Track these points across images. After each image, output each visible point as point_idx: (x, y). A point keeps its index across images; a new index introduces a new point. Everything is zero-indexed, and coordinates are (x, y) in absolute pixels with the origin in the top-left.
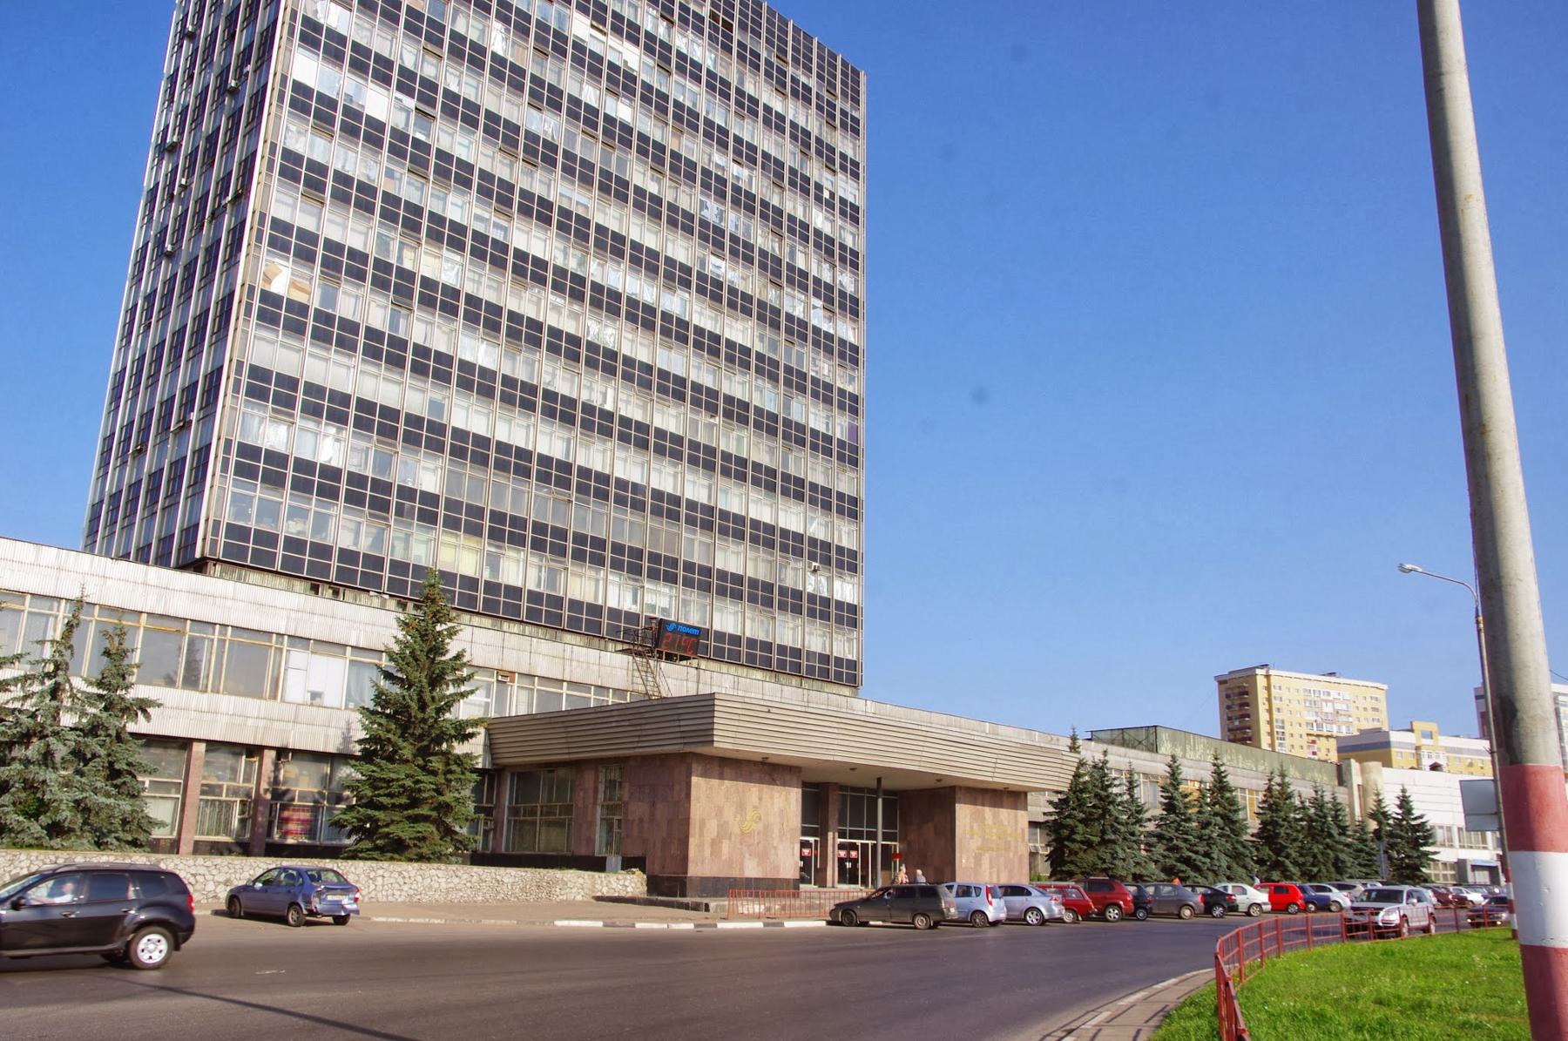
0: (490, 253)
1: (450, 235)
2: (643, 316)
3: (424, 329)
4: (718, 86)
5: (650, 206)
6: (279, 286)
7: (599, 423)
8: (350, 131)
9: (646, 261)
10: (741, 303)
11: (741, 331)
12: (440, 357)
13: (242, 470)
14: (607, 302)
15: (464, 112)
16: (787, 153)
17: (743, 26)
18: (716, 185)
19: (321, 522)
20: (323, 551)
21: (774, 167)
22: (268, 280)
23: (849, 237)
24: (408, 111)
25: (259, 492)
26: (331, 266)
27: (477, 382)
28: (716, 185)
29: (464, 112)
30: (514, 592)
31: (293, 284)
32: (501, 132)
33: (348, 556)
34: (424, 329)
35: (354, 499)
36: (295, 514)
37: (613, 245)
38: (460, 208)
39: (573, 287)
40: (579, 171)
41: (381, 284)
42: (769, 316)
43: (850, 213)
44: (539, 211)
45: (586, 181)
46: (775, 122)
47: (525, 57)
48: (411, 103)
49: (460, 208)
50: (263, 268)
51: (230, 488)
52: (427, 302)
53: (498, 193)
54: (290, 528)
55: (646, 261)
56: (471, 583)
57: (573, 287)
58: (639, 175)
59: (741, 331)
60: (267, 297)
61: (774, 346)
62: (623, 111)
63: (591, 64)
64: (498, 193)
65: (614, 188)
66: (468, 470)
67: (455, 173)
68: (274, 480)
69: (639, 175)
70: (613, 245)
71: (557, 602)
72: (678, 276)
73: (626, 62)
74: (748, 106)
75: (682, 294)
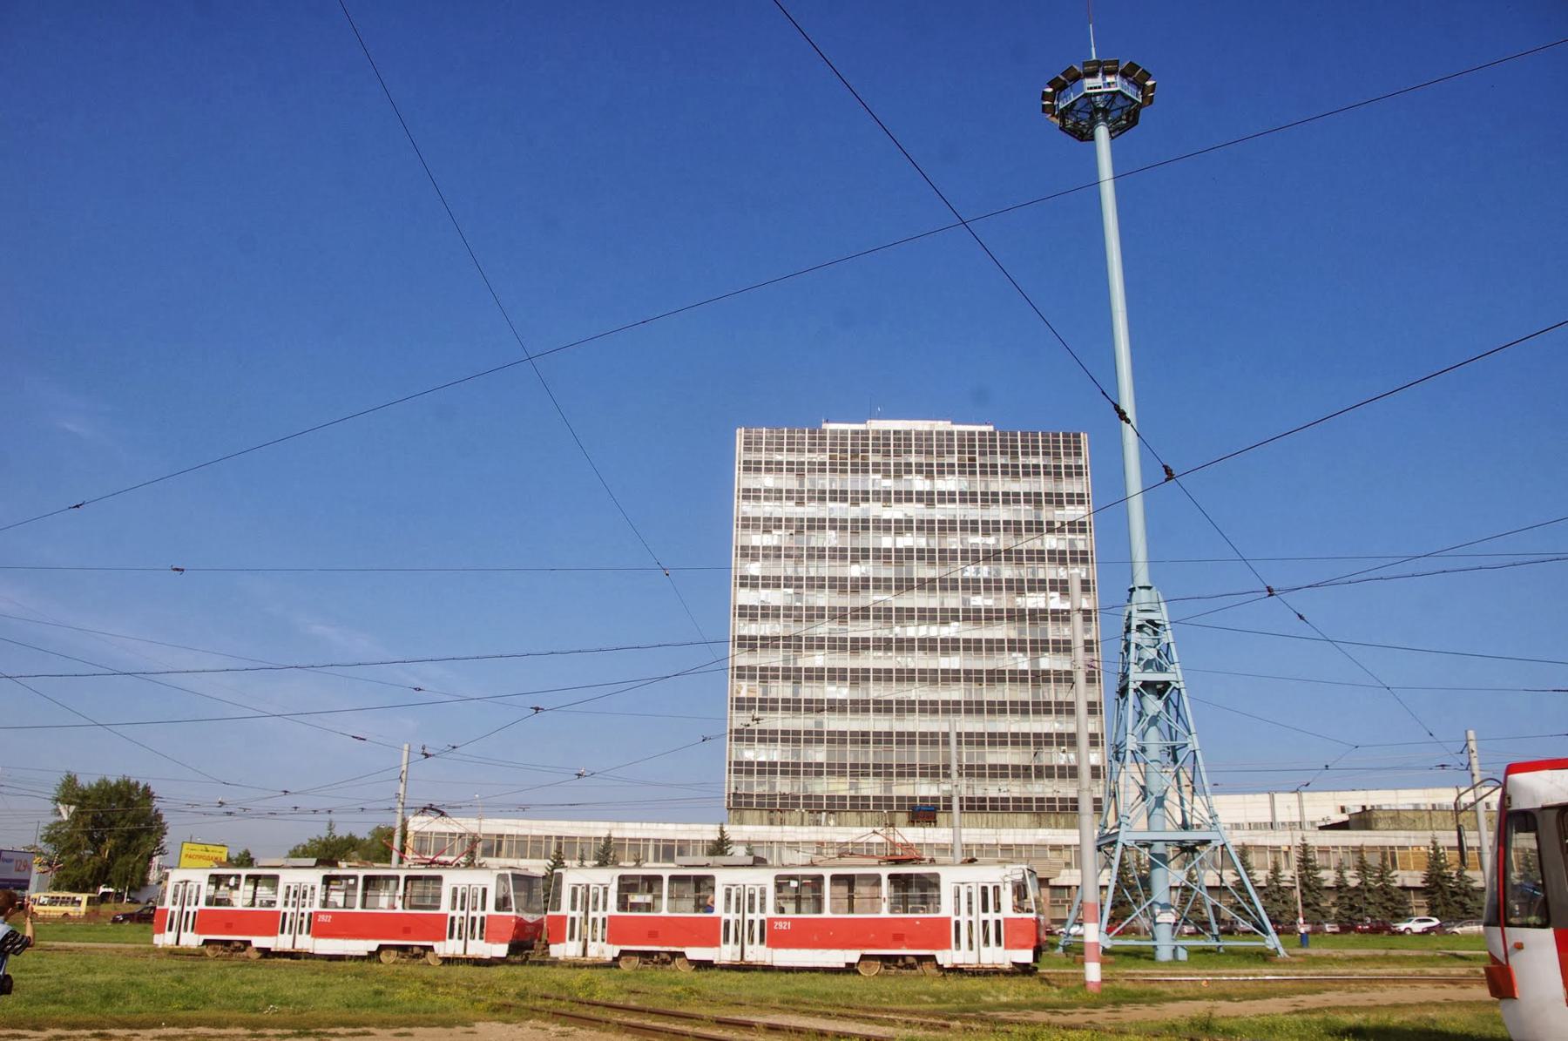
0: (837, 645)
1: (817, 644)
2: (928, 645)
3: (807, 691)
4: (968, 497)
5: (927, 585)
6: (744, 694)
7: (906, 707)
8: (765, 616)
9: (927, 616)
10: (993, 616)
11: (1002, 631)
12: (818, 701)
13: (736, 772)
14: (904, 645)
15: (816, 583)
16: (1024, 512)
17: (983, 454)
18: (970, 555)
19: (773, 786)
20: (773, 797)
21: (1014, 527)
22: (738, 692)
23: (1081, 542)
24: (791, 595)
25: (744, 778)
26: (764, 678)
27: (836, 707)
28: (970, 555)
29: (816, 583)
30: (866, 798)
31: (749, 691)
32: (838, 584)
33: (784, 796)
34: (807, 691)
35: (783, 773)
36: (760, 784)
37: (906, 615)
38: (823, 629)
39: (885, 645)
40: (881, 584)
41: (786, 678)
42: (1015, 615)
43: (1077, 527)
44: (862, 614)
45: (888, 588)
46: (1009, 498)
47: (848, 541)
48: (791, 591)
49: (823, 629)
50: (735, 688)
51: (733, 779)
52: (809, 678)
53: (840, 615)
54: (756, 790)
55: (927, 616)
56: (844, 798)
57: (885, 645)
58: (921, 571)
59: (1002, 631)
60: (738, 700)
61: (1021, 631)
62: (907, 541)
63: (884, 526)
64: (840, 615)
65: (904, 585)
66: (837, 747)
67: (815, 614)
68: (750, 773)
69: (921, 571)
70: (906, 615)
71: (890, 799)
72: (948, 616)
73: (906, 515)
74: (989, 498)
75: (956, 624)
